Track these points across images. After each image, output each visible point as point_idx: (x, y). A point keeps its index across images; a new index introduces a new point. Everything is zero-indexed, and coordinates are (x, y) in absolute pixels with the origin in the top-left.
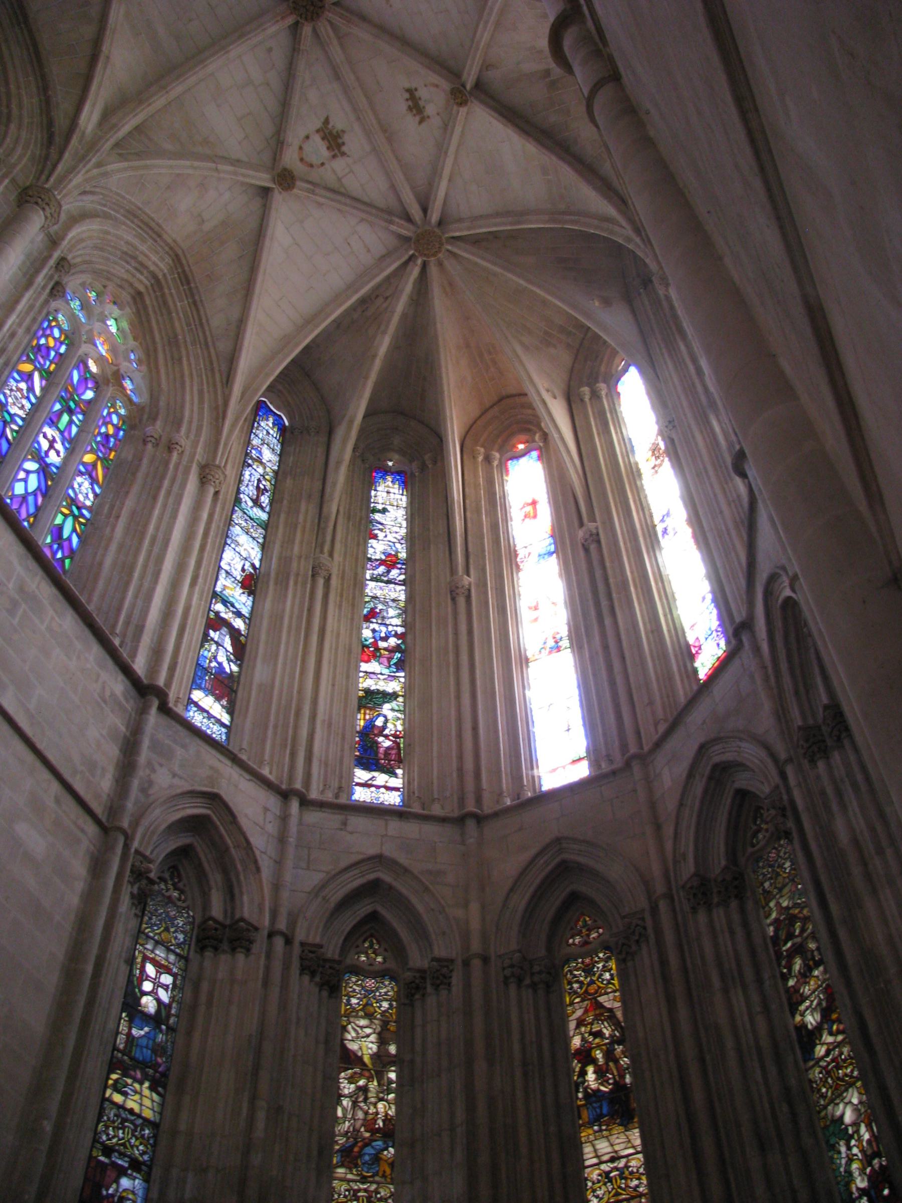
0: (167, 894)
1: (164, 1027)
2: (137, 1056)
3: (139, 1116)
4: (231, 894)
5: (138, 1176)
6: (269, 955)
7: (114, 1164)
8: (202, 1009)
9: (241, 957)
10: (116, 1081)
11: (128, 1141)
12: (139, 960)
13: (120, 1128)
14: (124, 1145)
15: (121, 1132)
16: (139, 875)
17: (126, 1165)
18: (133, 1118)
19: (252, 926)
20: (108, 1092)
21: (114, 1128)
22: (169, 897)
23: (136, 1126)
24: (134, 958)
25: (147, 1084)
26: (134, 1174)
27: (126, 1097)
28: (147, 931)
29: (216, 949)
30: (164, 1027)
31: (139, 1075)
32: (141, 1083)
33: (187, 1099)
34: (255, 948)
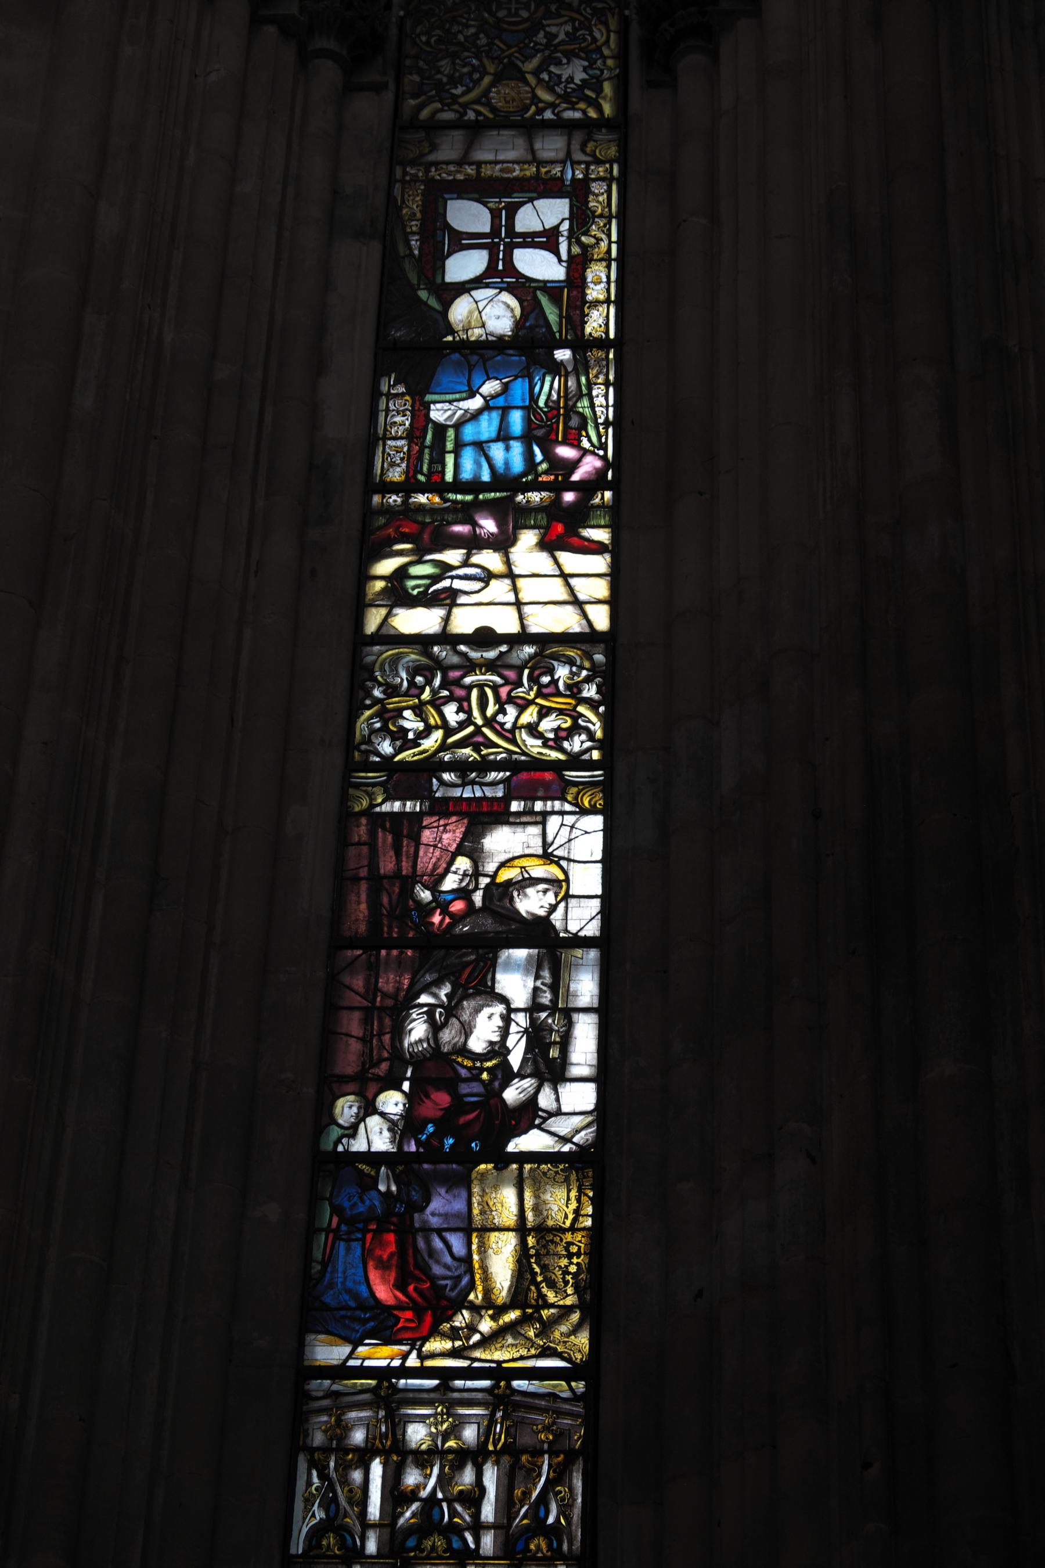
1: (563, 355)
3: (523, 637)
5: (557, 805)
10: (401, 573)
18: (491, 654)
21: (419, 711)
24: (393, 208)
25: (528, 538)
27: (453, 604)
28: (425, 113)
31: (489, 525)
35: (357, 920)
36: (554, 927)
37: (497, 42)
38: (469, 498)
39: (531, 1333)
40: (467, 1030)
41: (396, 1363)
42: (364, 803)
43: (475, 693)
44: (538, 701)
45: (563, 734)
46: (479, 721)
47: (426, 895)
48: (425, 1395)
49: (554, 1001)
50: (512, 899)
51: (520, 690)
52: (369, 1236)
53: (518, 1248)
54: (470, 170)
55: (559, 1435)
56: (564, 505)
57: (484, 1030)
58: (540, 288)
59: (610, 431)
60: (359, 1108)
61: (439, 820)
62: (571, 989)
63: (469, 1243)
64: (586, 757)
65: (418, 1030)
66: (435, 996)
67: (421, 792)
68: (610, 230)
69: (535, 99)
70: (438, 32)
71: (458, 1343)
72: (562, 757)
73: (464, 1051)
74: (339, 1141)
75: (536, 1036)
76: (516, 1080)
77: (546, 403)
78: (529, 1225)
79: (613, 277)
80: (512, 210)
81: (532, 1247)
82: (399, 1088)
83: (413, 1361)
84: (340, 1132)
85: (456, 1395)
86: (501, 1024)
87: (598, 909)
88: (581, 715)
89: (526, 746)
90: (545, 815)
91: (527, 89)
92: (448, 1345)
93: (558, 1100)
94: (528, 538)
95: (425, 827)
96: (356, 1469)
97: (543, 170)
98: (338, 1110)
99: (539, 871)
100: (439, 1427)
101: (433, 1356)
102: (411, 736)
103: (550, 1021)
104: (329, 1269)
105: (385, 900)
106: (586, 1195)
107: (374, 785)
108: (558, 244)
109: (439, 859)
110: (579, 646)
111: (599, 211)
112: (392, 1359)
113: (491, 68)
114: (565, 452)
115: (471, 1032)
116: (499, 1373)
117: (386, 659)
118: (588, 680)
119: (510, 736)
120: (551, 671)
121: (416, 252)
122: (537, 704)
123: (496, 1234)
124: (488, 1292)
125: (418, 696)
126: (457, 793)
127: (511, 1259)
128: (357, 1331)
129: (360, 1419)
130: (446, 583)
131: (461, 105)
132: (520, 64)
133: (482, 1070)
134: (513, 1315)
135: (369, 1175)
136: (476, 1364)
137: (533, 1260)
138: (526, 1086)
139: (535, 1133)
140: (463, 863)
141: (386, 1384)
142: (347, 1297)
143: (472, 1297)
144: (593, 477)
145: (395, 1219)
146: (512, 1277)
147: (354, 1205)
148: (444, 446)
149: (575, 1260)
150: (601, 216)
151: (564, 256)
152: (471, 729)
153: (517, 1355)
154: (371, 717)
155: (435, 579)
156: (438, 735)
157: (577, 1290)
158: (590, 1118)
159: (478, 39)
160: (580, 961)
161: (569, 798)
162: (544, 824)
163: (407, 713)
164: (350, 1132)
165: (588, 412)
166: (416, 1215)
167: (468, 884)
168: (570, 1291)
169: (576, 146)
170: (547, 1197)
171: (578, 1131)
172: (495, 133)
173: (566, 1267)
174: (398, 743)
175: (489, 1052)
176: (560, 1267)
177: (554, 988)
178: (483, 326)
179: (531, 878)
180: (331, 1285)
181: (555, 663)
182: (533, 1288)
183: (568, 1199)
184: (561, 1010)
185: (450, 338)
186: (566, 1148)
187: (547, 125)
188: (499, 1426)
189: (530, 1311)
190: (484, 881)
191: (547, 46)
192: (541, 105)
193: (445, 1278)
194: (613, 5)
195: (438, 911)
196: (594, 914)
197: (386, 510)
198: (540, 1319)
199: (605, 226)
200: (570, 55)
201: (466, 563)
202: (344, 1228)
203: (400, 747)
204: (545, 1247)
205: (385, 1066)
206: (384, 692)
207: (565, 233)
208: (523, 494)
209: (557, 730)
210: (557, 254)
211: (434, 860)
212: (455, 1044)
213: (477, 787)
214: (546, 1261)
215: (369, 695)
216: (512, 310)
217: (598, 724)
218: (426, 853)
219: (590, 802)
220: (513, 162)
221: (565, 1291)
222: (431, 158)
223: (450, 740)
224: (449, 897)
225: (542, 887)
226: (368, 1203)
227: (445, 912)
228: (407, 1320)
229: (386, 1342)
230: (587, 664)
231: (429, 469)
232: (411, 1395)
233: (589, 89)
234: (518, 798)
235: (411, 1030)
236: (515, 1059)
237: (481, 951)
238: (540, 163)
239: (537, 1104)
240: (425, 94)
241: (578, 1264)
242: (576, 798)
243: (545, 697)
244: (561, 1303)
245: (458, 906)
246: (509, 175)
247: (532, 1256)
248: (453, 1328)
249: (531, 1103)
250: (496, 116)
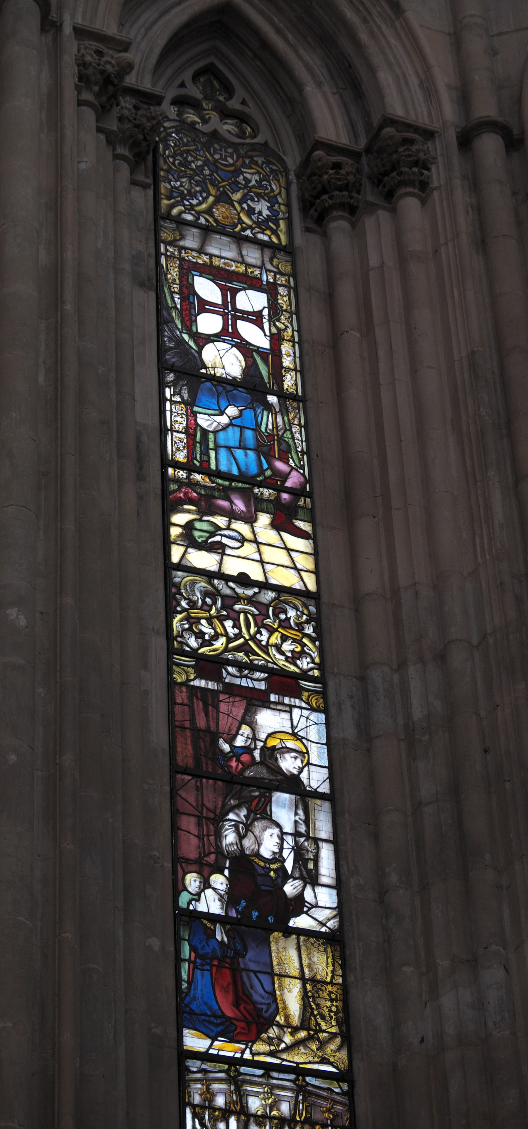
0: (206, 128)
1: (272, 399)
2: (223, 468)
3: (265, 586)
4: (353, 83)
5: (297, 702)
6: (474, 184)
7: (232, 690)
8: (352, 340)
9: (410, 206)
11: (253, 638)
12: (174, 274)
13: (227, 618)
14: (244, 648)
15: (228, 624)
16: (105, 87)
17: (262, 686)
18: (250, 592)
19: (417, 129)
20: (176, 553)
21: (210, 621)
22: (215, 135)
23: (263, 608)
24: (159, 273)
25: (264, 519)
26: (287, 700)
27: (223, 554)
28: (175, 211)
29: (352, 210)
30: (272, 399)
31: (240, 505)
32: (250, 520)
33: (366, 527)
34: (437, 175)
35: (186, 756)
36: (303, 782)
37: (215, 174)
38: (226, 483)
39: (314, 1048)
41: (238, 1055)
42: (183, 677)
43: (242, 616)
44: (280, 630)
45: (297, 655)
46: (247, 637)
47: (226, 747)
48: (256, 1079)
50: (277, 759)
51: (268, 620)
52: (214, 969)
53: (301, 990)
54: (206, 258)
55: (336, 1115)
56: (283, 502)
58: (255, 351)
59: (305, 457)
60: (200, 882)
61: (229, 698)
62: (317, 826)
63: (273, 983)
64: (311, 673)
65: (230, 837)
66: (238, 815)
67: (218, 678)
68: (292, 321)
69: (241, 221)
70: (179, 158)
71: (272, 1048)
72: (298, 671)
73: (258, 855)
74: (189, 903)
76: (291, 880)
77: (266, 429)
78: (307, 977)
79: (297, 355)
80: (234, 292)
81: (310, 991)
82: (222, 873)
83: (247, 1056)
84: (191, 896)
85: (275, 1082)
86: (278, 841)
87: (327, 776)
88: (306, 645)
89: (275, 658)
90: (291, 707)
91: (235, 212)
92: (266, 1048)
93: (315, 897)
94: (264, 519)
95: (221, 701)
96: (221, 1121)
97: (249, 270)
98: (187, 882)
99: (291, 744)
100: (267, 1101)
101: (259, 1054)
102: (207, 637)
104: (193, 987)
105: (202, 745)
106: (337, 962)
107: (188, 666)
108: (263, 323)
109: (232, 724)
110: (300, 598)
111: (285, 308)
112: (236, 1053)
113: (213, 191)
114: (280, 465)
115: (261, 844)
116: (297, 1070)
117: (187, 582)
118: (308, 622)
119: (266, 650)
120: (285, 612)
121: (179, 306)
122: (279, 632)
123: (288, 979)
124: (287, 1017)
125: (209, 611)
126: (237, 681)
127: (298, 997)
128: (213, 1031)
129: (221, 1089)
130: (217, 538)
131: (196, 211)
132: (230, 194)
134: (303, 1034)
135: (210, 928)
136: (284, 1063)
137: (311, 1000)
138: (297, 885)
139: (304, 916)
140: (245, 730)
141: (233, 1069)
142: (205, 1008)
143: (278, 1018)
144: (298, 487)
145: (228, 960)
146: (300, 1009)
147: (203, 946)
148: (208, 445)
149: (335, 1004)
150: (286, 311)
151: (268, 333)
152: (242, 640)
153: (307, 1060)
154: (182, 620)
155: (212, 534)
156: (223, 640)
157: (338, 1024)
158: (335, 913)
159: (204, 170)
160: (320, 808)
161: (304, 698)
162: (291, 712)
163: (203, 622)
164: (196, 897)
165: (291, 442)
166: (240, 959)
167: (250, 744)
168: (334, 1023)
169: (267, 260)
170: (315, 959)
171: (329, 920)
172: (218, 237)
173: (330, 1007)
174: (200, 641)
175: (273, 859)
176: (326, 1006)
177: (307, 822)
178: (224, 368)
179: (286, 747)
180: (194, 999)
181: (287, 607)
182: (313, 1018)
183: (328, 964)
184: (312, 838)
185: (204, 371)
186: (324, 929)
187: (247, 239)
188: (301, 1105)
189: (312, 1033)
190: (260, 744)
191: (246, 186)
192: (244, 225)
193: (261, 1004)
194: (282, 170)
195: (235, 759)
196: (325, 778)
197: (177, 480)
198: (318, 1039)
199: (289, 318)
200: (260, 196)
201: (228, 528)
202: (198, 961)
203: (201, 644)
204: (317, 992)
205: (213, 857)
206: (188, 604)
207: (267, 317)
208: (258, 488)
209: (293, 652)
210: (263, 329)
211: (229, 724)
212: (253, 850)
213: (249, 680)
214: (319, 1001)
215: (179, 605)
216: (240, 362)
217: (316, 653)
218: (223, 718)
219: (316, 703)
220: (231, 260)
221: (331, 1023)
222: (182, 243)
223: (231, 645)
224: (240, 751)
225: (293, 754)
226: (211, 946)
227: (238, 760)
228: (242, 1028)
229: (231, 1041)
230: (306, 612)
231: (201, 458)
232: (248, 1078)
233: (272, 222)
234: (274, 693)
235: (226, 836)
236: (289, 865)
237: (261, 790)
238: (248, 265)
239: (304, 898)
240: (174, 198)
241: (336, 1006)
242: (308, 699)
243: (284, 628)
244: (329, 1030)
245: (245, 758)
246: (229, 268)
247: (310, 997)
248: (269, 1037)
249: (300, 897)
250: (218, 225)
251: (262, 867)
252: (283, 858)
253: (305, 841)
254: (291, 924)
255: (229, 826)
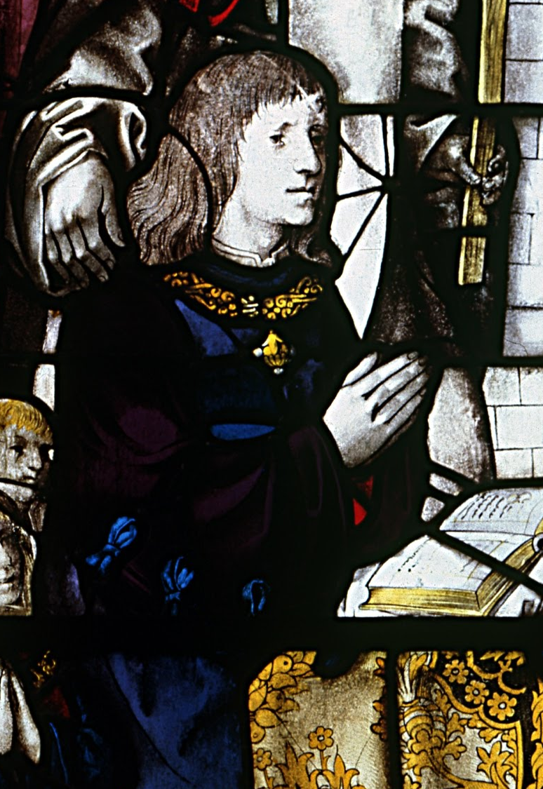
40: (216, 186)
49: (466, 77)
57: (265, 173)
65: (70, 189)
66: (115, 60)
75: (414, 192)
76: (367, 363)
93: (484, 432)
103: (455, 152)
115: (227, 193)
133: (262, 327)
138: (392, 385)
139: (424, 546)
212: (182, 234)
236: (358, 289)
251: (225, 323)
252: (334, 249)
253: (448, 133)
254: (353, 605)
255: (67, 128)
